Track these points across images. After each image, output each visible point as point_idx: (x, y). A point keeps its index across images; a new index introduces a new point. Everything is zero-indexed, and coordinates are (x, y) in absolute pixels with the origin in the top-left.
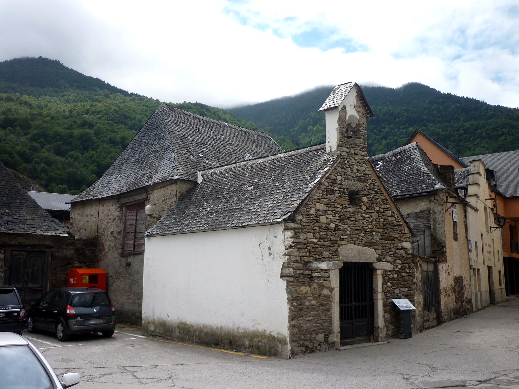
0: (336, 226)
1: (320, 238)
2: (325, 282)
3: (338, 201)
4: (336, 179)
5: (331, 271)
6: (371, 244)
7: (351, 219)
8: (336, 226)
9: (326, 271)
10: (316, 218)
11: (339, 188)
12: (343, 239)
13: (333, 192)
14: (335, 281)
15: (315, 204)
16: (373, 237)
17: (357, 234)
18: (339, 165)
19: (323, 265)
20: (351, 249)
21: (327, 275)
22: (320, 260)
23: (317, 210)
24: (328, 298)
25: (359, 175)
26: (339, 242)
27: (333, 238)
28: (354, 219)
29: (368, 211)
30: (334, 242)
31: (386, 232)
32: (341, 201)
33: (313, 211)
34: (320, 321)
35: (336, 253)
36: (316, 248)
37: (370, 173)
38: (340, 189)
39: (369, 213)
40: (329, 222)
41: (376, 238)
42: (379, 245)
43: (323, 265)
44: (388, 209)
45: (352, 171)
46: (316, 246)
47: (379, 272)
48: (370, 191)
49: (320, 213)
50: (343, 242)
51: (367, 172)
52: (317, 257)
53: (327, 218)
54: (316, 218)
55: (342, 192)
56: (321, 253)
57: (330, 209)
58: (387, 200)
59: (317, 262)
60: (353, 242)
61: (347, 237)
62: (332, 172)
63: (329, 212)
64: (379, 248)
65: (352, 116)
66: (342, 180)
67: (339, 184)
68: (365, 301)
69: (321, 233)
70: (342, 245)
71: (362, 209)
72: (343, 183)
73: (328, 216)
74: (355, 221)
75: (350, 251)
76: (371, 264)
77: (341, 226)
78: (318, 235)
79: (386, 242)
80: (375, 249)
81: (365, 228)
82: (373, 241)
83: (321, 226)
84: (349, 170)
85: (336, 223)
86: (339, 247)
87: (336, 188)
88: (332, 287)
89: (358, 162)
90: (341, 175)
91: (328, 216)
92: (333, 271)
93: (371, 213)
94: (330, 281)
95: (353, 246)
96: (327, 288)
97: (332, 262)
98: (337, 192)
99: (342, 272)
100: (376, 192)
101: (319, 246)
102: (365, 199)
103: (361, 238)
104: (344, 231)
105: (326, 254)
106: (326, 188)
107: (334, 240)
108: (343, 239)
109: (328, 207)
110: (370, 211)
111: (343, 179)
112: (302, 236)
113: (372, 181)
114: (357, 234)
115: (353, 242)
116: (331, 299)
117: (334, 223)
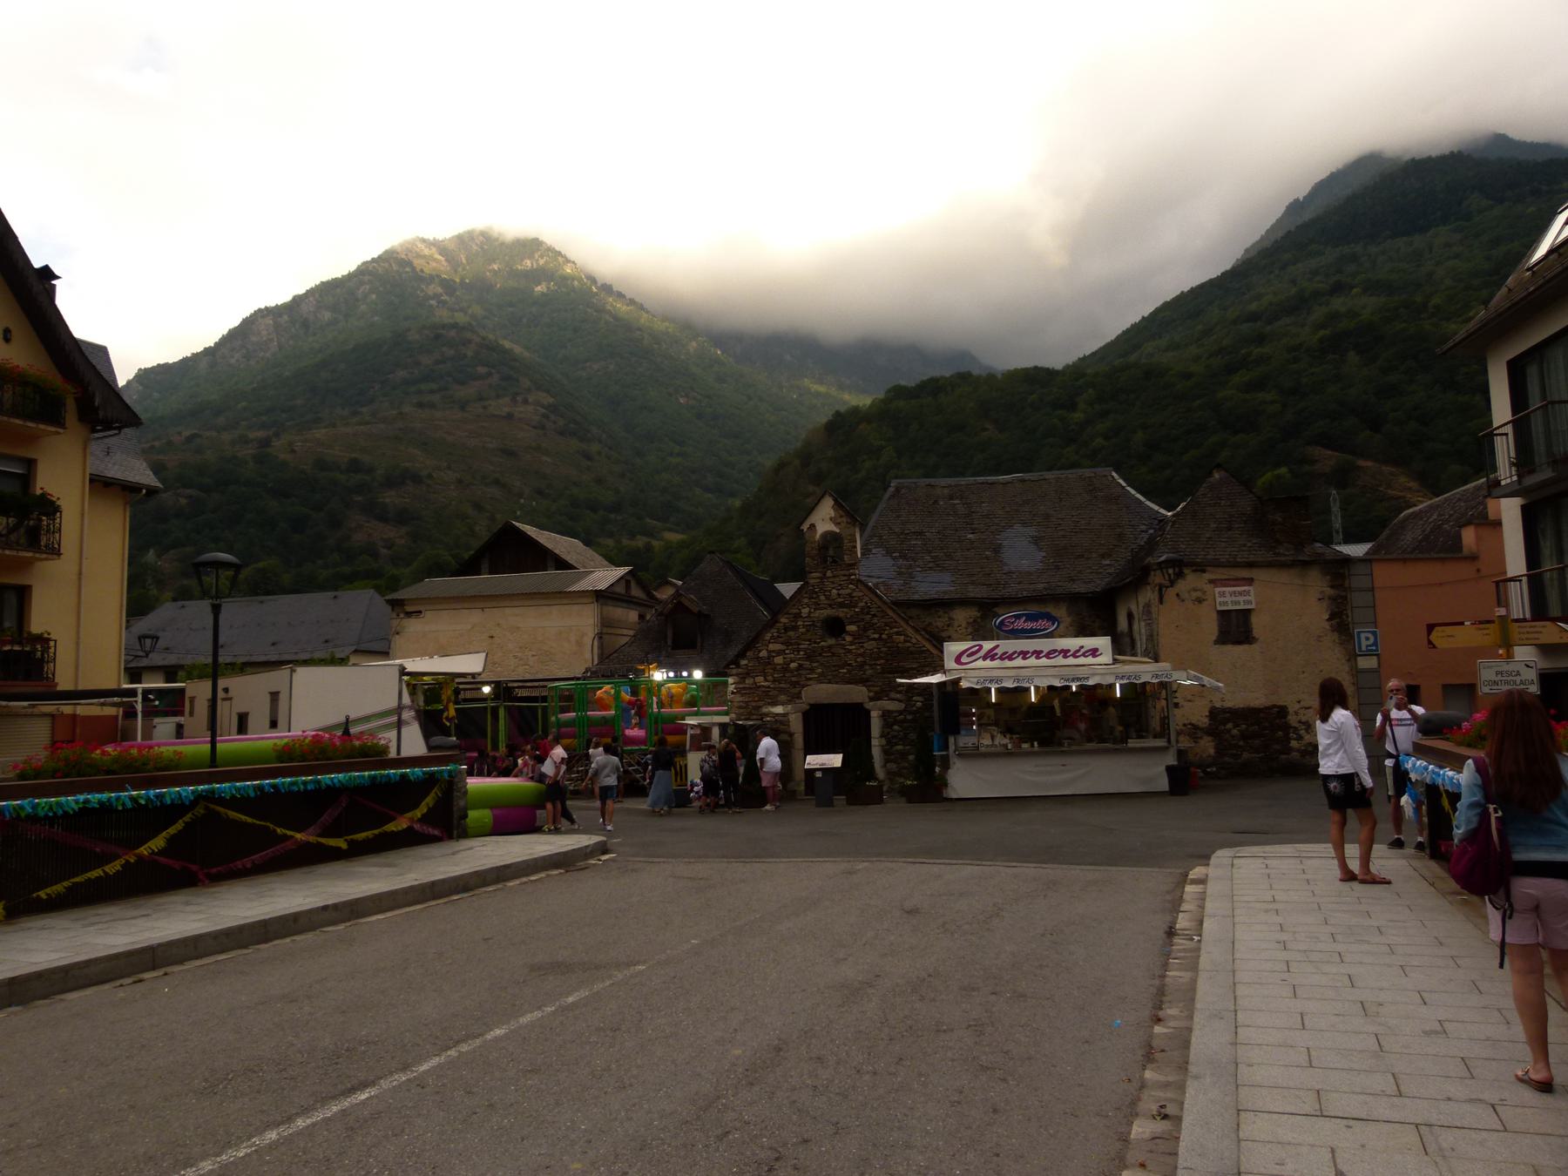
6: (862, 681)
13: (795, 628)
19: (779, 709)
22: (774, 704)
30: (794, 684)
32: (808, 636)
33: (764, 654)
41: (869, 672)
43: (779, 709)
44: (898, 633)
45: (828, 598)
47: (874, 714)
65: (826, 535)
76: (861, 704)
95: (824, 686)
105: (783, 698)
112: (749, 681)
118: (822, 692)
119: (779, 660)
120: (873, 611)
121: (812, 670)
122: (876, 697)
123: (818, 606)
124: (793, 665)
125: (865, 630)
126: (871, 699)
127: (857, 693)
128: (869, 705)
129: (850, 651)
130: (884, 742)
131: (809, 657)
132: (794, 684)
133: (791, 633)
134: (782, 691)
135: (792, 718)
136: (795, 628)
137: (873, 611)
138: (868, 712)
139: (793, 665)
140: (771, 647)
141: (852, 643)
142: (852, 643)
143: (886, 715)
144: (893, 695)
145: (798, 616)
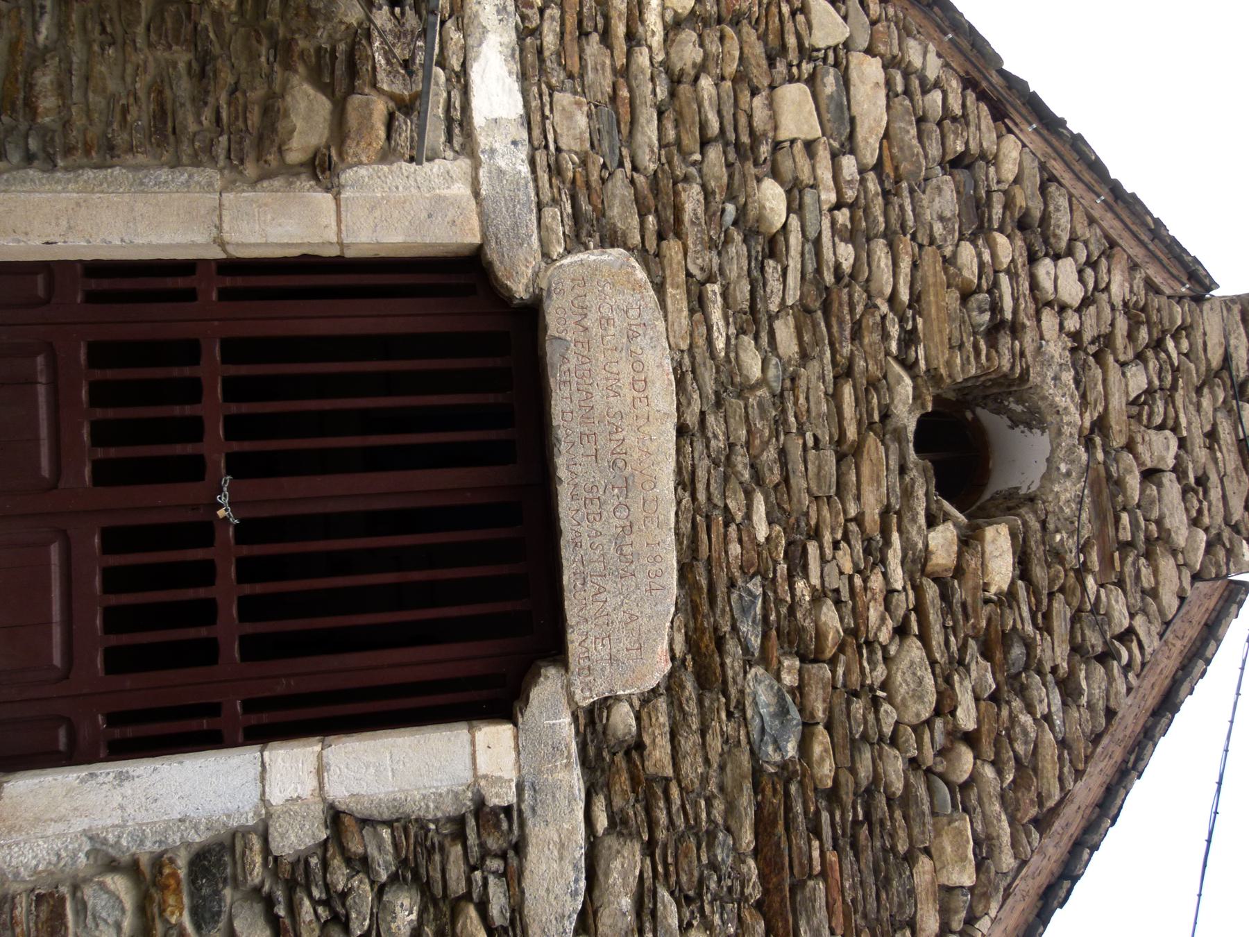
0: (772, 241)
1: (675, 81)
2: (380, 108)
3: (932, 268)
4: (1057, 257)
5: (464, 163)
7: (847, 391)
8: (773, 246)
9: (459, 125)
10: (791, 41)
11: (1012, 274)
12: (698, 304)
14: (394, 207)
15: (870, 51)
16: (764, 660)
17: (758, 478)
18: (1139, 283)
19: (495, 92)
20: (641, 383)
21: (435, 134)
22: (531, 67)
23: (839, 56)
24: (252, 147)
25: (1133, 482)
26: (673, 248)
27: (692, 199)
28: (851, 433)
29: (932, 591)
31: (816, 831)
34: (76, 43)
35: (589, 228)
36: (606, 37)
37: (1169, 600)
38: (1004, 280)
39: (920, 608)
40: (786, 165)
41: (761, 691)
42: (715, 744)
43: (495, 92)
44: (984, 849)
46: (620, 29)
48: (1061, 611)
49: (830, 83)
50: (677, 296)
51: (1167, 565)
52: (550, 40)
53: (809, 146)
54: (791, 41)
55: (995, 308)
56: (576, 78)
57: (873, 186)
58: (1042, 823)
59: (511, 37)
60: (692, 420)
61: (720, 344)
62: (1092, 221)
63: (849, 165)
64: (689, 742)
66: (1063, 308)
67: (1034, 285)
68: (253, 649)
69: (706, 83)
70: (660, 288)
71: (932, 522)
72: (1049, 320)
73: (823, 155)
74: (840, 458)
75: (625, 369)
77: (786, 286)
78: (689, 52)
79: (747, 838)
80: (672, 684)
81: (812, 548)
82: (732, 646)
83: (754, 92)
84: (1138, 380)
85: (795, 239)
86: (650, 259)
87: (1001, 239)
88: (348, 176)
89: (1202, 481)
90: (1086, 302)
91: (823, 155)
92: (461, 190)
93: (924, 638)
94: (387, 155)
95: (663, 399)
96: (340, 129)
97: (525, 169)
98: (987, 257)
99: (467, 272)
100: (1068, 689)
101: (621, 61)
102: (999, 565)
103: (736, 505)
104: (753, 319)
105: (573, 123)
106: (983, 156)
107: (678, 209)
108: (698, 304)
109: (878, 167)
110: (937, 638)
111: (1072, 323)
113: (1128, 635)
114: (758, 478)
115: (692, 420)
116: (250, 170)
117: (794, 222)
118: (621, 383)
119: (796, 113)
120: (1092, 682)
121: (753, 319)
122: (602, 750)
123: (1090, 353)
124: (772, 197)
125: (993, 644)
126: (591, 721)
127: (623, 618)
128: (551, 705)
129: (875, 555)
130: (298, 836)
131: (824, 300)
132: (659, 200)
133: (943, 199)
134: (616, 115)
135: (444, 178)
136: (977, 225)
137: (1092, 682)
138: (499, 700)
139: (772, 197)
140: (867, 72)
141: (917, 563)
142: (917, 563)
143: (492, 829)
144: (625, 865)
145: (1037, 236)
